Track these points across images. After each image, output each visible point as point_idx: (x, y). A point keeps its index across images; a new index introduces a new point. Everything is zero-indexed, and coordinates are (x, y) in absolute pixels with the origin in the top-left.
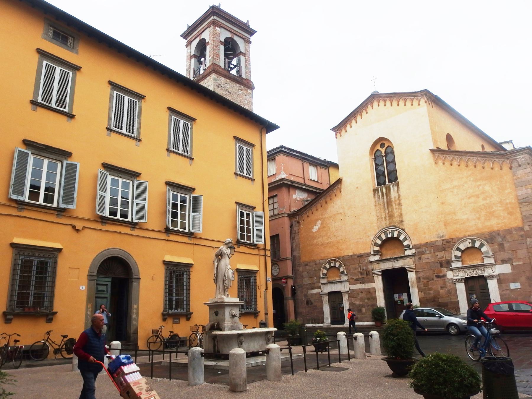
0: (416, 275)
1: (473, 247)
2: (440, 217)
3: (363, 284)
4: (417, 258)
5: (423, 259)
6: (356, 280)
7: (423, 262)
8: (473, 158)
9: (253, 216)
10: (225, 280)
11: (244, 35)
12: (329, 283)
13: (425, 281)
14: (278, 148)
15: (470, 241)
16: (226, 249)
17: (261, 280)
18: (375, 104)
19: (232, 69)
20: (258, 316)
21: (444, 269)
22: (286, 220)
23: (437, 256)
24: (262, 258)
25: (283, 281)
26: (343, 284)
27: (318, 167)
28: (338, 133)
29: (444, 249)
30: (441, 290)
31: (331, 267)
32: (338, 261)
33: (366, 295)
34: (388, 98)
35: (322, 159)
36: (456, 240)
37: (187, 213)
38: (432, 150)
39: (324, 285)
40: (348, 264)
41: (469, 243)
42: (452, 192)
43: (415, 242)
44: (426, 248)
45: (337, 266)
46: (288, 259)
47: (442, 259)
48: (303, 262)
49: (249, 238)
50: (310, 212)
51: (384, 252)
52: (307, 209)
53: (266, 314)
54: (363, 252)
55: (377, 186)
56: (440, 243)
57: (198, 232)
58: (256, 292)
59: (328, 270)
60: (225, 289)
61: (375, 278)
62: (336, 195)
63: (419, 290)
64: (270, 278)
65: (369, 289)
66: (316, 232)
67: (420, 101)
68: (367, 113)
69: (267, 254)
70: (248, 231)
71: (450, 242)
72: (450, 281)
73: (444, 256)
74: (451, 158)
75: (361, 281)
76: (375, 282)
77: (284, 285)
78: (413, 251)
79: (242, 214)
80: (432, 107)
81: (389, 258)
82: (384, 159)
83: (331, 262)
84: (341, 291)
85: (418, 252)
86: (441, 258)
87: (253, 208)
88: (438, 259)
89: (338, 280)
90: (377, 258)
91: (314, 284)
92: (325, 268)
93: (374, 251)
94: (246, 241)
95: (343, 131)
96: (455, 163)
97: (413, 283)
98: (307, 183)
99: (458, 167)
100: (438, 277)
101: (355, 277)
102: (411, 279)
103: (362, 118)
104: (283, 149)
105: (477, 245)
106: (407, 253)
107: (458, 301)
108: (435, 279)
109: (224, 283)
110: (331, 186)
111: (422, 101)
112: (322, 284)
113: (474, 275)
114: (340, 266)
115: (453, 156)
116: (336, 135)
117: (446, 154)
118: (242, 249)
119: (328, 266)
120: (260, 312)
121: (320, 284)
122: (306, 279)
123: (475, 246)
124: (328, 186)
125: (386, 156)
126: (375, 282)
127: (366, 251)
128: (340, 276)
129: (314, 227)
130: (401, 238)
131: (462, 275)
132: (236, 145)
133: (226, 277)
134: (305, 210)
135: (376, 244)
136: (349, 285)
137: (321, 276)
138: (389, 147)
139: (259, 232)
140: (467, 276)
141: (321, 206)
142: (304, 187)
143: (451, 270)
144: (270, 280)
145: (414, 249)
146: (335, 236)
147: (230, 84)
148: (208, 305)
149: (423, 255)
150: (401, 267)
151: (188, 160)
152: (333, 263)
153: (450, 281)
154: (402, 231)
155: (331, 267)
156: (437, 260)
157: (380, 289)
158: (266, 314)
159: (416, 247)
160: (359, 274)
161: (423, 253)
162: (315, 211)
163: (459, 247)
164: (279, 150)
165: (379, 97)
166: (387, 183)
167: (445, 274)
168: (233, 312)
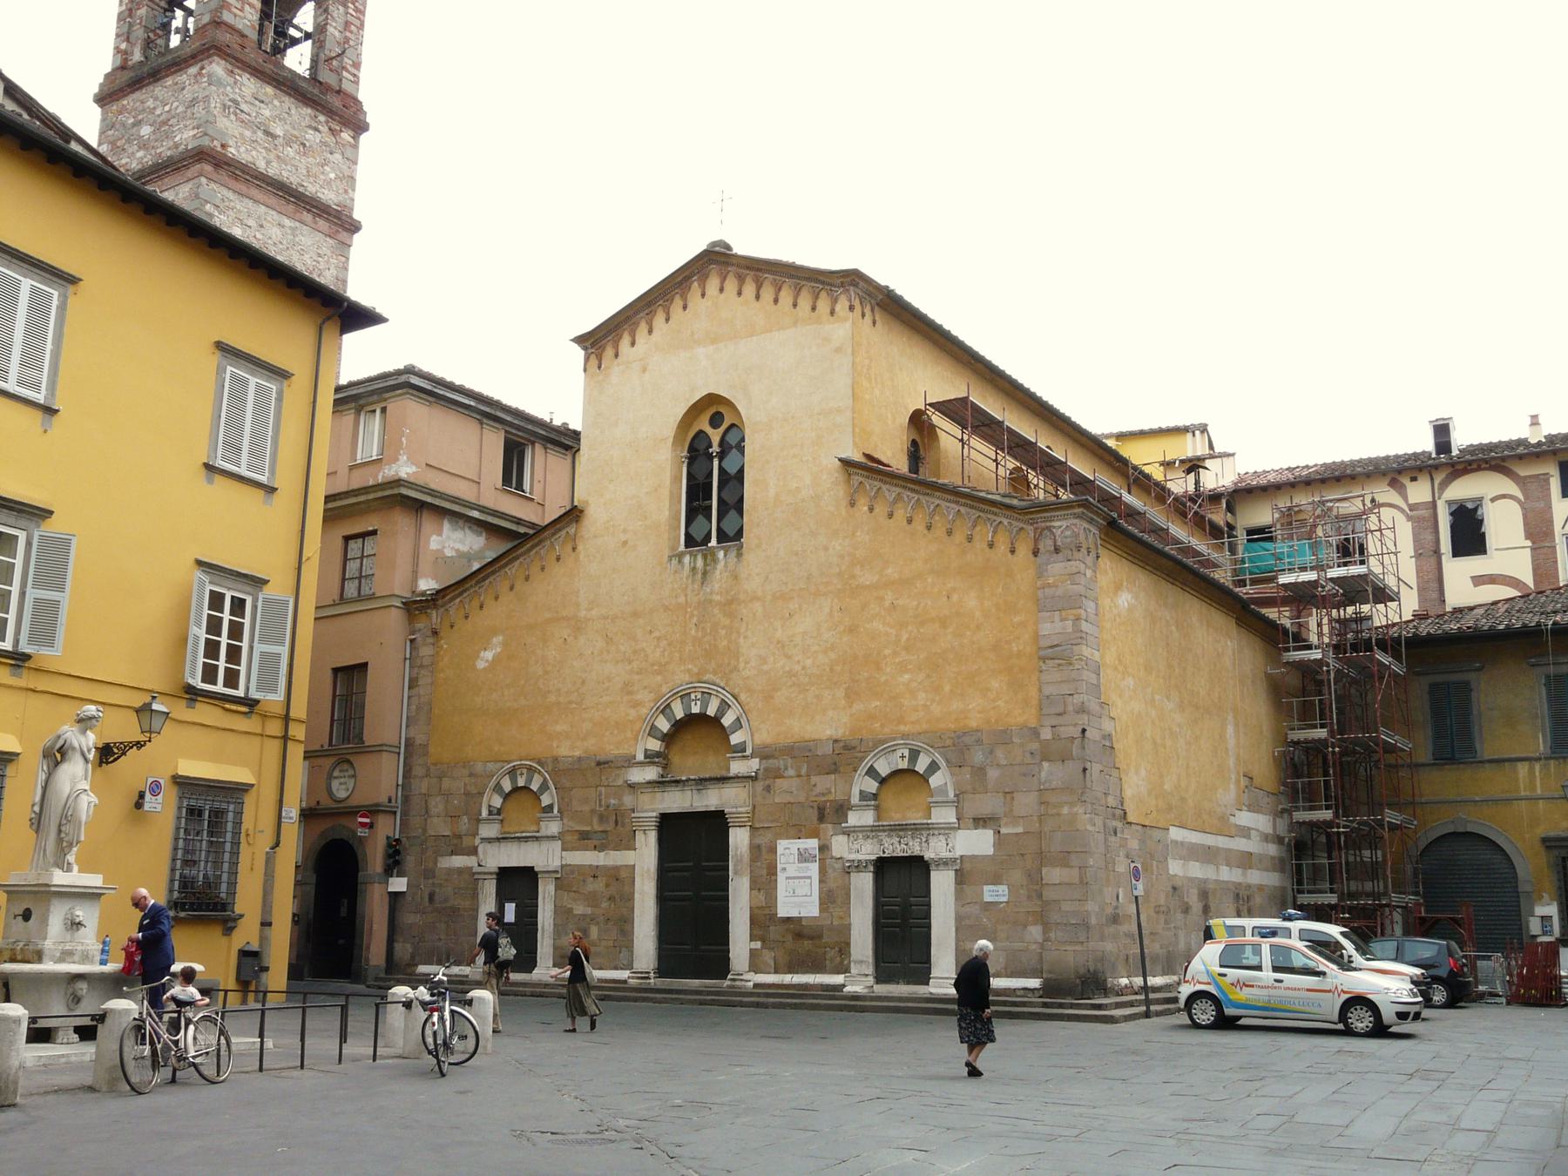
0: (752, 837)
2: (838, 668)
3: (603, 851)
4: (760, 785)
6: (584, 836)
8: (948, 504)
9: (255, 607)
10: (64, 822)
14: (398, 373)
15: (906, 753)
16: (78, 735)
17: (256, 817)
18: (713, 283)
19: (295, 42)
20: (232, 929)
22: (394, 619)
23: (815, 785)
24: (274, 747)
25: (360, 820)
26: (545, 845)
28: (593, 357)
29: (833, 769)
32: (540, 772)
33: (607, 885)
34: (752, 273)
35: (557, 422)
37: (15, 589)
38: (847, 463)
39: (489, 846)
40: (568, 785)
41: (903, 757)
42: (882, 599)
46: (385, 748)
48: (435, 764)
49: (232, 679)
50: (476, 603)
51: (675, 759)
52: (465, 591)
53: (266, 924)
55: (682, 547)
56: (828, 749)
57: (45, 651)
58: (235, 853)
60: (63, 849)
61: (639, 836)
62: (558, 559)
64: (292, 812)
65: (617, 868)
66: (485, 669)
68: (685, 308)
69: (291, 733)
70: (234, 654)
71: (854, 748)
72: (837, 866)
73: (833, 790)
74: (894, 495)
76: (635, 849)
77: (361, 832)
78: (754, 764)
79: (216, 601)
80: (874, 323)
81: (684, 778)
82: (716, 462)
83: (519, 772)
84: (536, 869)
85: (766, 770)
86: (823, 795)
87: (258, 582)
88: (816, 796)
90: (651, 773)
91: (460, 837)
92: (498, 788)
94: (219, 688)
95: (609, 352)
96: (901, 514)
97: (739, 861)
99: (908, 527)
102: (737, 849)
103: (667, 320)
104: (415, 380)
105: (921, 767)
106: (737, 767)
107: (850, 924)
109: (60, 831)
111: (842, 306)
112: (483, 839)
113: (901, 854)
114: (544, 787)
115: (898, 490)
116: (587, 359)
117: (881, 481)
118: (205, 713)
119: (507, 786)
120: (241, 916)
121: (477, 841)
122: (435, 820)
125: (722, 455)
126: (635, 849)
127: (624, 750)
128: (540, 820)
129: (482, 654)
130: (727, 721)
131: (868, 851)
132: (221, 371)
133: (69, 813)
134: (461, 594)
135: (653, 731)
136: (563, 850)
137: (485, 813)
138: (735, 429)
139: (269, 661)
141: (512, 588)
142: (475, 514)
143: (844, 833)
144: (291, 818)
145: (758, 760)
147: (276, 102)
151: (38, 415)
152: (524, 777)
153: (838, 866)
154: (730, 699)
155: (516, 790)
156: (813, 799)
157: (649, 870)
158: (266, 924)
159: (763, 753)
160: (595, 820)
161: (777, 774)
162: (490, 602)
163: (875, 766)
164: (403, 379)
165: (727, 264)
166: (713, 542)
168: (78, 913)
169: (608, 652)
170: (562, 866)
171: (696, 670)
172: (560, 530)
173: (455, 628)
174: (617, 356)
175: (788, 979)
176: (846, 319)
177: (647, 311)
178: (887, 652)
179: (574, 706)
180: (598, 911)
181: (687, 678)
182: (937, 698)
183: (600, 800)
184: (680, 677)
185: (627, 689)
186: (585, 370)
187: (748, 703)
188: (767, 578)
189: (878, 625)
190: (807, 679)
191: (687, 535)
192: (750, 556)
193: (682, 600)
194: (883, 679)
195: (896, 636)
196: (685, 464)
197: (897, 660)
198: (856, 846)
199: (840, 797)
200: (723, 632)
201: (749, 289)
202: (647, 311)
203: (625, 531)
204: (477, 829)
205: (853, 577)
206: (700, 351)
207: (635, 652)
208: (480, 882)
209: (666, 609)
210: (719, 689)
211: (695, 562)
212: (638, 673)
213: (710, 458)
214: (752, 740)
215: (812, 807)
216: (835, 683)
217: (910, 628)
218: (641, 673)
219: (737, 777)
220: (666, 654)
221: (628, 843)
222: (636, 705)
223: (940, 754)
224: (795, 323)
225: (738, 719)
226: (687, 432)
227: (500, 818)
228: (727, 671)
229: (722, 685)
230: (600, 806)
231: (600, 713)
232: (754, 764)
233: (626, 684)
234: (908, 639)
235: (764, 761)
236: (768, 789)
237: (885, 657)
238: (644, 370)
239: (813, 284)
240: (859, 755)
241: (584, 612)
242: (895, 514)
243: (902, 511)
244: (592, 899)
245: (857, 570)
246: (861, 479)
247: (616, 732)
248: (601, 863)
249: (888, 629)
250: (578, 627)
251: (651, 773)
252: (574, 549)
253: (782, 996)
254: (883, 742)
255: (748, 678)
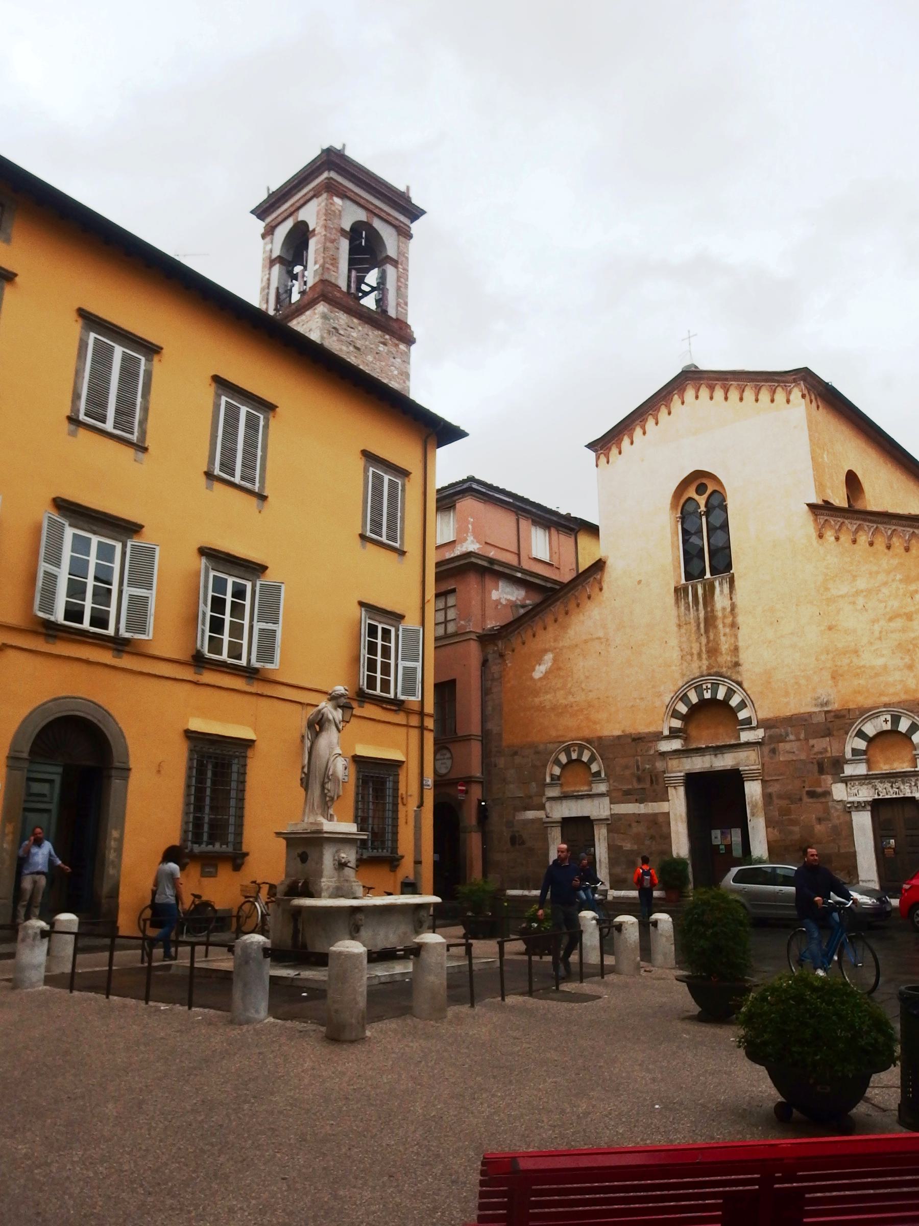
0: (764, 788)
1: (894, 732)
2: (823, 657)
4: (766, 749)
5: (779, 753)
6: (627, 793)
7: (781, 759)
9: (397, 636)
10: (326, 780)
11: (397, 219)
12: (565, 797)
13: (783, 803)
14: (464, 481)
15: (889, 718)
16: (332, 710)
17: (408, 783)
18: (690, 394)
19: (366, 294)
20: (397, 866)
21: (829, 779)
22: (474, 648)
23: (813, 746)
24: (414, 733)
25: (460, 788)
26: (596, 801)
27: (553, 531)
28: (602, 457)
29: (828, 733)
30: (818, 826)
31: (570, 761)
33: (648, 828)
34: (720, 383)
35: (563, 512)
36: (857, 713)
37: (246, 623)
38: (811, 506)
40: (611, 756)
41: (886, 721)
42: (854, 603)
43: (764, 713)
44: (789, 729)
45: (585, 758)
46: (473, 737)
47: (824, 756)
49: (385, 685)
50: (530, 633)
51: (693, 732)
53: (418, 862)
54: (646, 730)
55: (683, 581)
56: (821, 718)
57: (269, 666)
58: (395, 811)
59: (563, 767)
60: (326, 803)
61: (671, 791)
62: (589, 597)
63: (769, 823)
64: (429, 781)
65: (656, 815)
66: (540, 679)
67: (790, 392)
68: (669, 413)
69: (426, 724)
70: (386, 669)
71: (844, 716)
74: (855, 527)
75: (636, 797)
76: (669, 801)
77: (461, 797)
78: (760, 734)
79: (372, 631)
80: (818, 407)
81: (704, 746)
82: (704, 519)
83: (572, 749)
84: (592, 818)
85: (771, 737)
87: (400, 617)
88: (815, 754)
89: (586, 791)
90: (676, 744)
91: (530, 797)
92: (557, 762)
93: (670, 728)
94: (378, 692)
95: (614, 451)
96: (863, 539)
97: (754, 806)
98: (526, 565)
99: (870, 549)
100: (812, 794)
101: (625, 787)
102: (752, 797)
103: (657, 424)
104: (475, 486)
105: (904, 726)
106: (746, 736)
108: (806, 799)
110: (579, 576)
111: (796, 394)
113: (894, 796)
114: (592, 759)
115: (858, 522)
116: (598, 458)
117: (844, 517)
118: (370, 710)
119: (563, 759)
120: (402, 857)
121: (544, 800)
122: (512, 786)
123: (899, 729)
124: (574, 575)
125: (707, 514)
126: (669, 801)
127: (652, 729)
128: (590, 783)
129: (537, 667)
130: (734, 702)
131: (865, 794)
132: (366, 471)
133: (330, 773)
134: (518, 628)
135: (675, 714)
136: (611, 803)
137: (548, 780)
138: (716, 495)
139: (409, 674)
140: (876, 797)
141: (556, 621)
142: (519, 575)
143: (842, 782)
144: (428, 785)
145: (762, 730)
146: (583, 690)
147: (360, 328)
148: (284, 838)
149: (781, 745)
150: (729, 768)
151: (254, 501)
152: (576, 753)
153: (839, 807)
154: (735, 687)
155: (570, 761)
156: (812, 757)
157: (681, 816)
158: (418, 862)
159: (765, 724)
160: (635, 781)
161: (782, 739)
162: (540, 632)
163: (863, 729)
164: (465, 486)
165: (700, 379)
166: (708, 575)
167: (829, 790)
168: (343, 855)
170: (611, 815)
173: (516, 651)
196: (680, 523)
204: (544, 792)
208: (549, 829)
215: (812, 763)
225: (743, 700)
227: (560, 782)
235: (768, 731)
239: (770, 384)
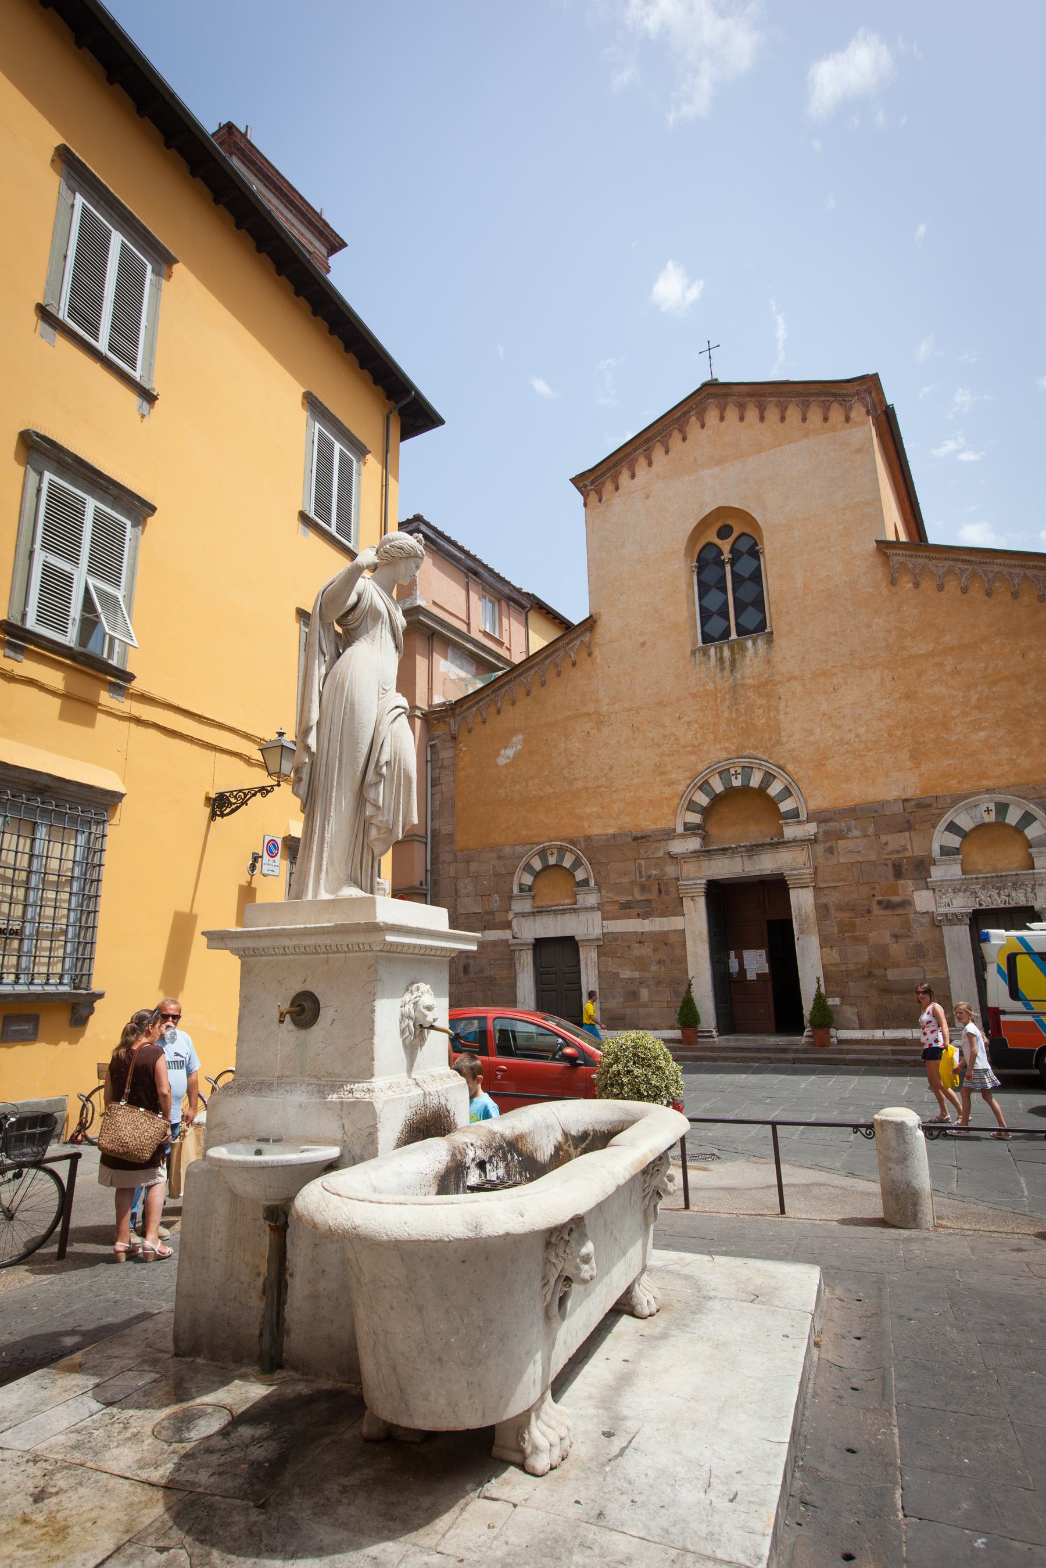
0: (816, 897)
1: (1000, 824)
2: (898, 732)
3: (648, 918)
4: (820, 848)
5: (839, 853)
6: (626, 906)
7: (841, 861)
8: (1010, 570)
11: (311, 243)
12: (538, 912)
13: (845, 916)
15: (992, 806)
18: (712, 416)
21: (907, 885)
23: (886, 844)
26: (583, 917)
27: (503, 603)
29: (908, 826)
30: (895, 945)
31: (546, 868)
32: (571, 851)
33: (655, 950)
34: (754, 400)
36: (949, 801)
39: (523, 920)
40: (604, 860)
41: (988, 811)
42: (941, 664)
43: (819, 801)
44: (853, 822)
45: (567, 863)
46: (416, 838)
47: (901, 855)
48: (462, 851)
50: (493, 710)
51: (713, 830)
52: (481, 700)
54: (653, 827)
55: (700, 644)
56: (898, 808)
59: (537, 875)
61: (687, 903)
63: (825, 942)
65: (665, 933)
66: (506, 764)
67: (850, 408)
68: (684, 439)
71: (930, 805)
72: (923, 920)
73: (909, 847)
75: (638, 911)
76: (684, 915)
78: (812, 828)
81: (733, 846)
82: (728, 568)
83: (549, 852)
84: (577, 938)
85: (825, 832)
86: (898, 852)
88: (889, 854)
89: (567, 905)
90: (694, 844)
91: (492, 913)
92: (528, 868)
93: (685, 824)
95: (609, 486)
98: (475, 635)
100: (888, 905)
101: (623, 899)
102: (800, 909)
105: (1013, 817)
106: (791, 832)
107: (948, 978)
108: (877, 910)
109: (361, 799)
110: (529, 658)
112: (517, 915)
114: (577, 863)
119: (537, 865)
121: (510, 916)
123: (1007, 821)
124: (524, 657)
126: (684, 915)
127: (662, 825)
129: (502, 752)
131: (962, 904)
133: (385, 757)
135: (692, 806)
136: (603, 919)
137: (516, 890)
140: (978, 907)
141: (528, 694)
145: (814, 824)
146: (565, 778)
148: (235, 951)
149: (841, 842)
150: (768, 872)
151: (134, 400)
152: (555, 856)
153: (925, 920)
155: (546, 868)
156: (886, 857)
157: (701, 934)
159: (818, 817)
160: (636, 891)
161: (840, 835)
165: (726, 395)
166: (734, 636)
167: (908, 898)
169: (635, 739)
170: (604, 934)
171: (734, 748)
172: (574, 639)
174: (617, 489)
175: (878, 1034)
176: (864, 423)
177: (644, 448)
178: (955, 713)
179: (603, 789)
180: (647, 975)
181: (725, 755)
182: (1024, 752)
183: (640, 872)
184: (716, 753)
185: (659, 769)
186: (585, 505)
187: (796, 773)
188: (804, 658)
189: (939, 689)
190: (862, 745)
191: (703, 633)
192: (780, 642)
193: (710, 686)
194: (954, 738)
195: (964, 697)
196: (695, 573)
197: (968, 720)
198: (945, 900)
199: (918, 852)
200: (761, 711)
201: (752, 414)
202: (644, 448)
203: (642, 634)
204: (510, 906)
205: (905, 648)
206: (706, 473)
207: (664, 737)
208: (517, 953)
209: (694, 696)
210: (762, 762)
211: (721, 652)
212: (669, 755)
213: (722, 565)
214: (806, 806)
215: (886, 865)
216: (896, 747)
217: (979, 688)
218: (673, 755)
219: (795, 841)
220: (699, 736)
221: (676, 909)
222: (671, 783)
223: (1035, 804)
224: (806, 435)
225: (786, 788)
226: (695, 545)
227: (532, 893)
228: (769, 746)
229: (764, 758)
230: (641, 876)
231: (632, 793)
232: (812, 828)
233: (657, 766)
234: (978, 699)
235: (823, 824)
236: (830, 850)
237: (954, 718)
238: (647, 497)
239: (822, 398)
240: (937, 811)
241: (606, 707)
242: (946, 587)
243: (955, 583)
244: (641, 964)
245: (908, 642)
246: (902, 559)
247: (651, 809)
248: (647, 929)
249: (953, 691)
250: (600, 720)
251: (694, 844)
252: (590, 655)
253: (868, 1052)
254: (965, 797)
255: (794, 750)
